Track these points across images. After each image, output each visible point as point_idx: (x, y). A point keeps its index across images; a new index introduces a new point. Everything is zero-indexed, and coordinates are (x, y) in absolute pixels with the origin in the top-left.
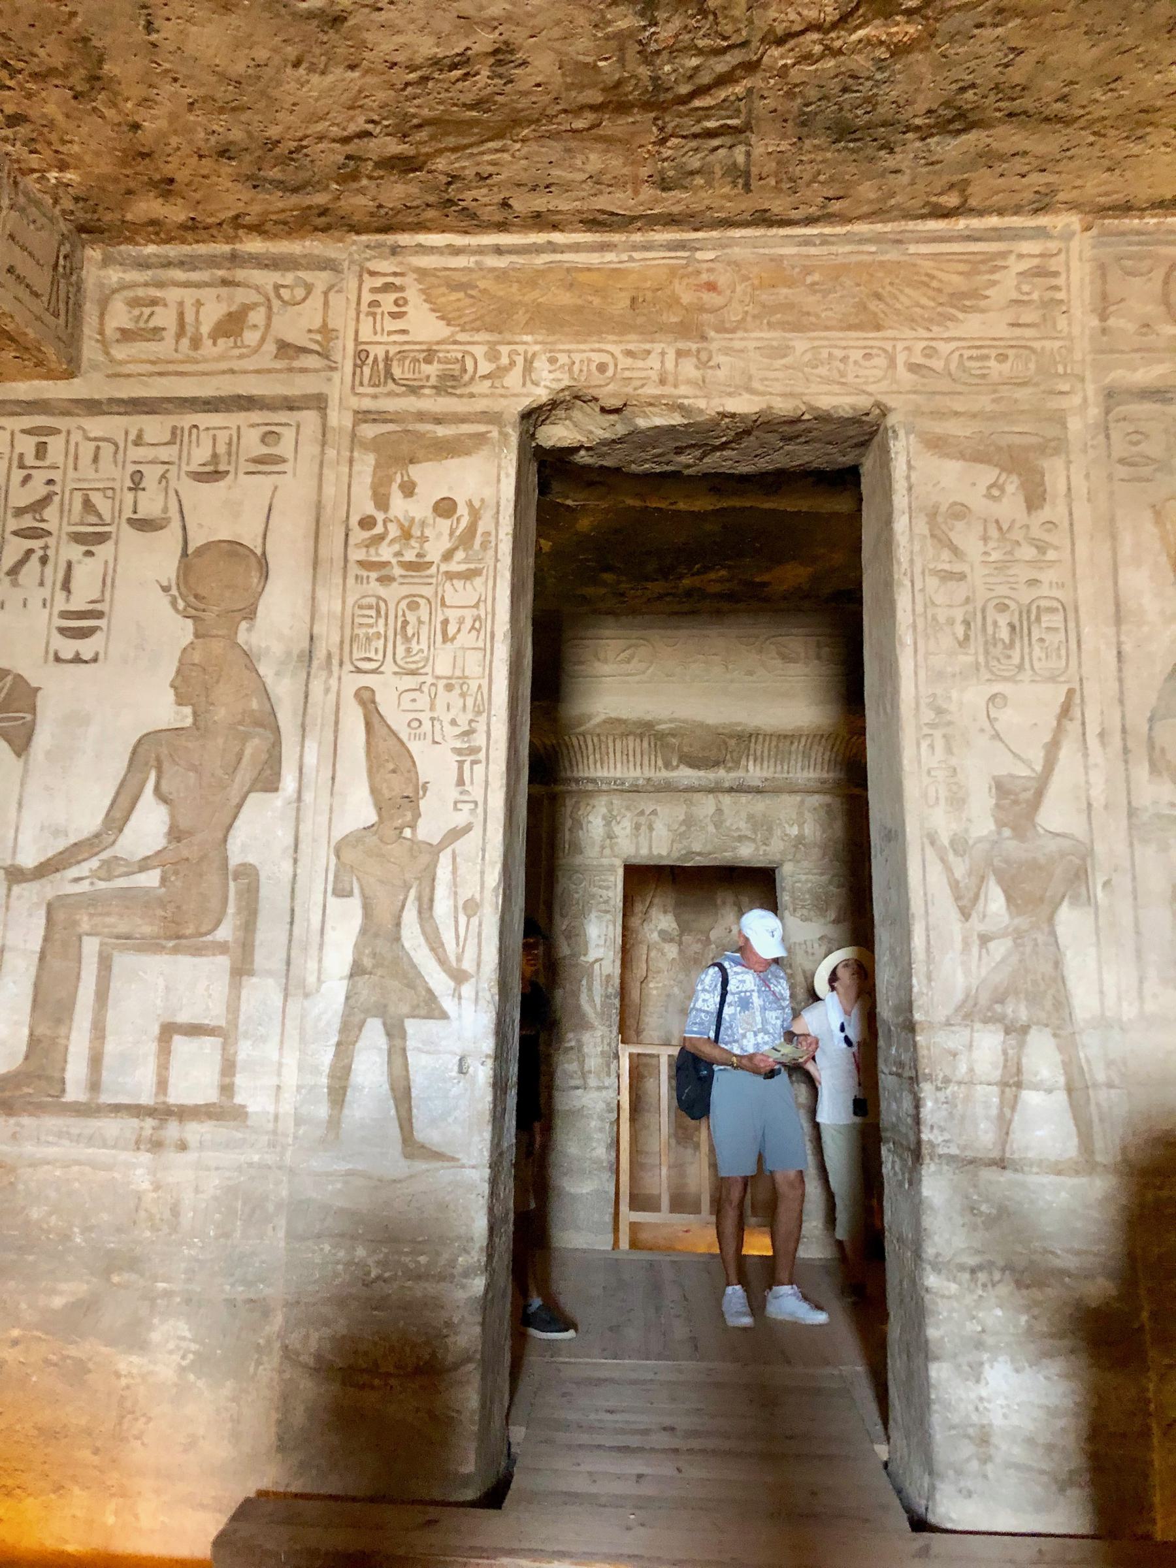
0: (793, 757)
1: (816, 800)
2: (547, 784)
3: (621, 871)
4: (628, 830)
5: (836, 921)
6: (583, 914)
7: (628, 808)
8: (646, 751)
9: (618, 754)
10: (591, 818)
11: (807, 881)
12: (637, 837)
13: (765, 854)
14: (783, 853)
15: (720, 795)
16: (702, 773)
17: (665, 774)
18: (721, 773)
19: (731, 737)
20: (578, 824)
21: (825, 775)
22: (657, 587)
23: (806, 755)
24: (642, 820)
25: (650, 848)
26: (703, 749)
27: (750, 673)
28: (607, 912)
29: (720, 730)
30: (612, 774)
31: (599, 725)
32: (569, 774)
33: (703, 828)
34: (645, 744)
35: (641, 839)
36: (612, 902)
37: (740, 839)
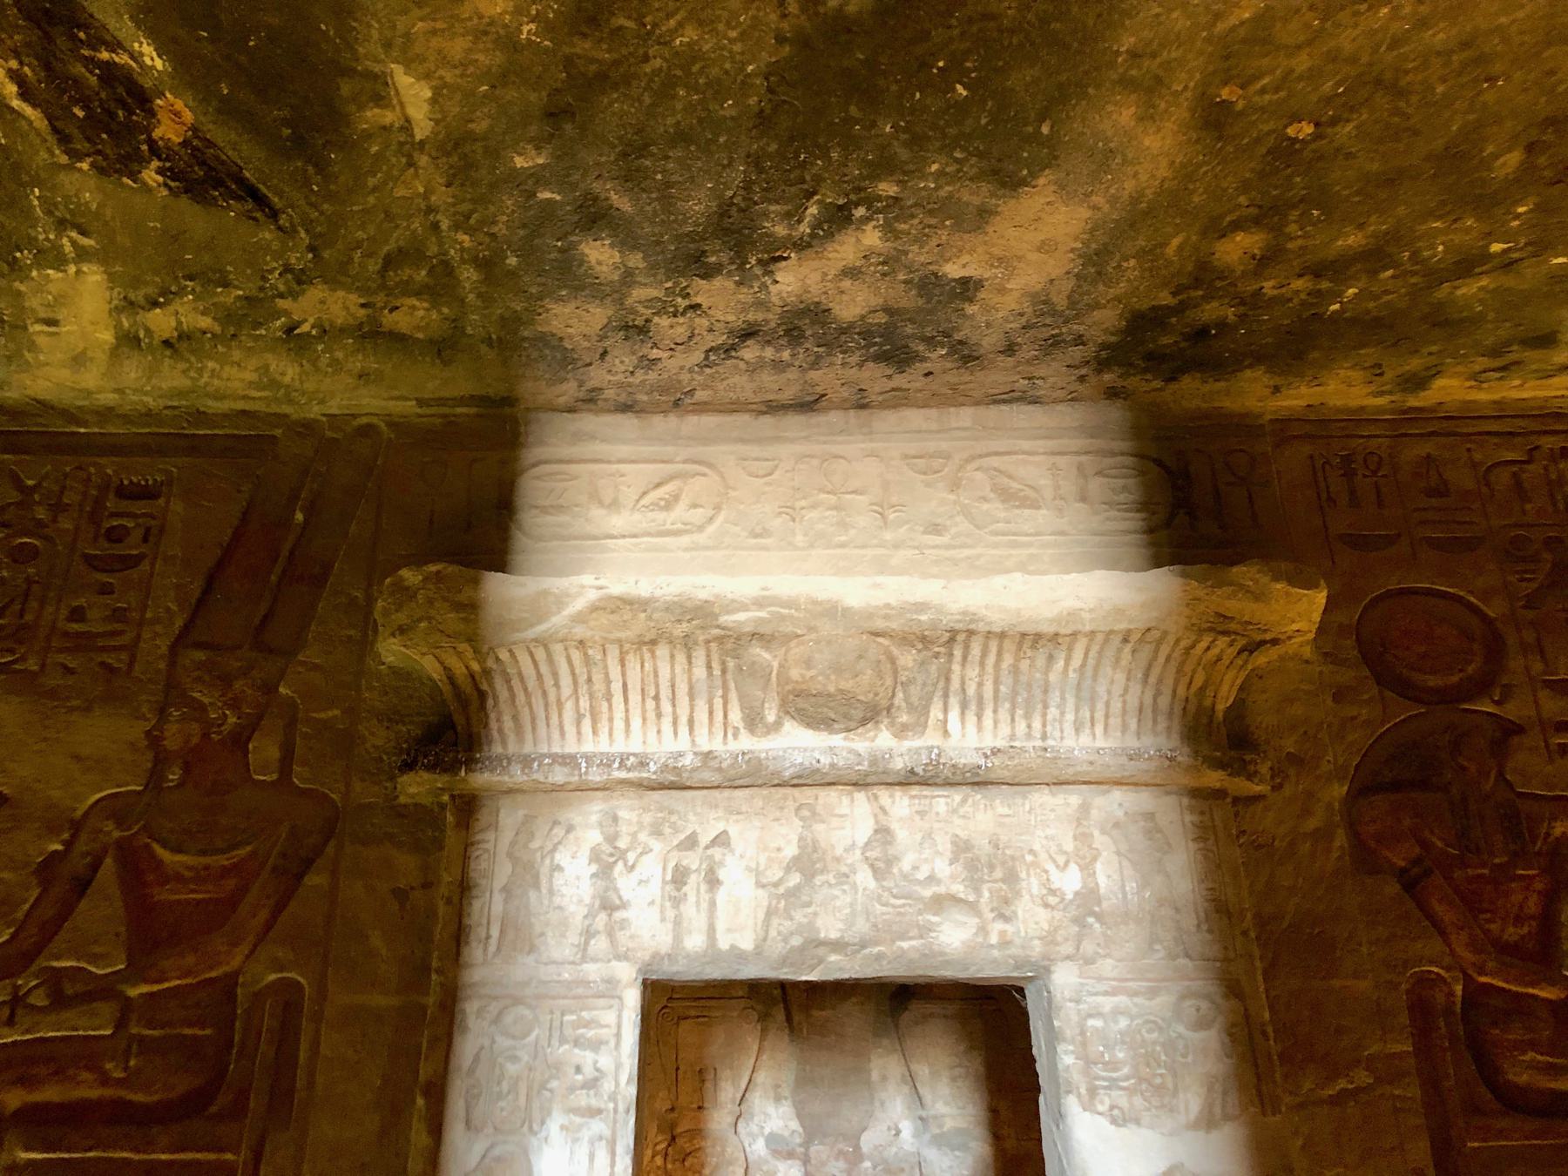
0: (1055, 698)
1: (1115, 802)
2: (452, 768)
3: (632, 999)
4: (655, 889)
5: (1207, 1122)
6: (530, 1122)
7: (657, 832)
8: (702, 687)
9: (635, 697)
10: (562, 857)
11: (1117, 1012)
12: (677, 902)
13: (1005, 943)
14: (1049, 939)
15: (884, 795)
16: (837, 740)
17: (746, 742)
18: (882, 740)
19: (905, 640)
20: (528, 874)
21: (1132, 742)
22: (721, 299)
23: (1085, 695)
24: (692, 860)
25: (711, 931)
26: (838, 669)
27: (936, 529)
28: (593, 1112)
29: (880, 624)
30: (620, 746)
31: (579, 618)
32: (512, 748)
33: (844, 877)
34: (700, 672)
35: (689, 909)
36: (607, 1086)
37: (941, 903)
